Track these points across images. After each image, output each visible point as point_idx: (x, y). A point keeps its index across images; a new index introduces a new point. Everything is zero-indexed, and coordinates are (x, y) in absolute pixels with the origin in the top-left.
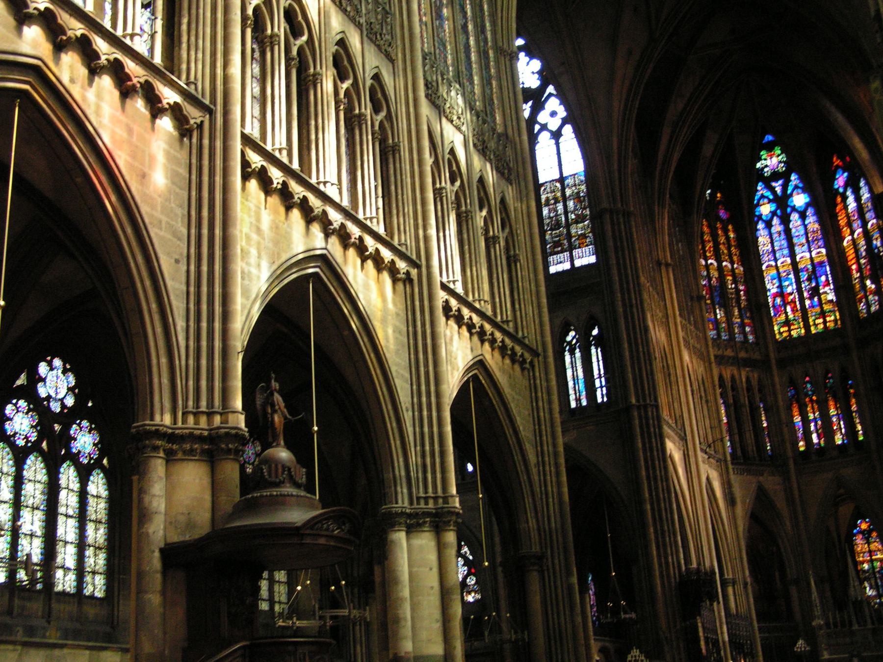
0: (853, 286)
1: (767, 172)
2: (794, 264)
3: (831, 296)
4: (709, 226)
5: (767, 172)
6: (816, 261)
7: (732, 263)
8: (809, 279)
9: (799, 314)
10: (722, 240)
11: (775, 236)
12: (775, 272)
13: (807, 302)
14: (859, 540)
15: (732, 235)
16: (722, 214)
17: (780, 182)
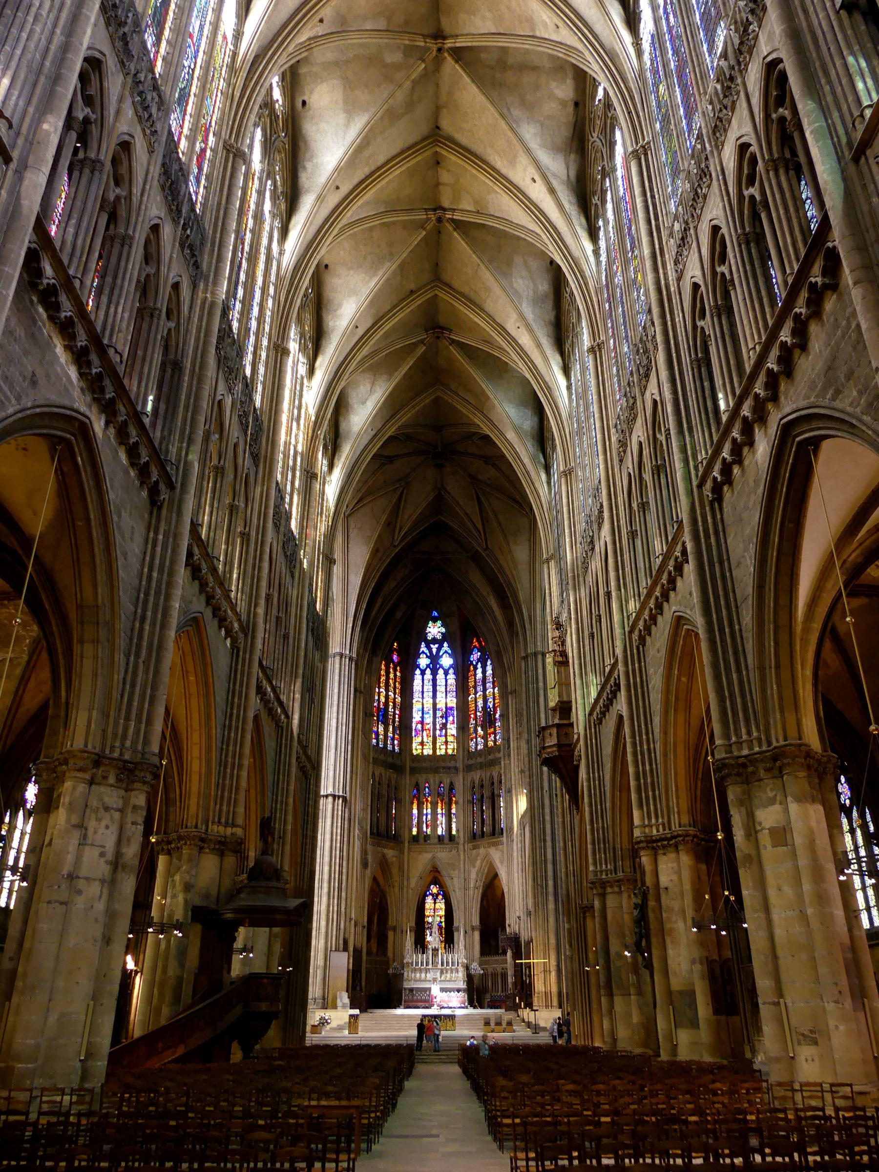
0: (469, 729)
1: (430, 637)
2: (435, 704)
3: (454, 732)
4: (385, 666)
5: (430, 637)
6: (449, 705)
7: (395, 694)
8: (442, 717)
9: (431, 739)
10: (392, 676)
11: (426, 682)
12: (421, 707)
13: (438, 732)
14: (429, 900)
15: (398, 674)
16: (395, 657)
17: (437, 646)
